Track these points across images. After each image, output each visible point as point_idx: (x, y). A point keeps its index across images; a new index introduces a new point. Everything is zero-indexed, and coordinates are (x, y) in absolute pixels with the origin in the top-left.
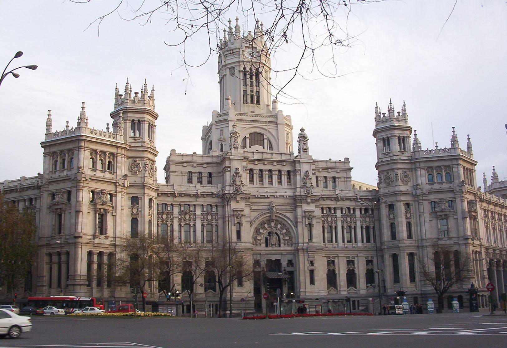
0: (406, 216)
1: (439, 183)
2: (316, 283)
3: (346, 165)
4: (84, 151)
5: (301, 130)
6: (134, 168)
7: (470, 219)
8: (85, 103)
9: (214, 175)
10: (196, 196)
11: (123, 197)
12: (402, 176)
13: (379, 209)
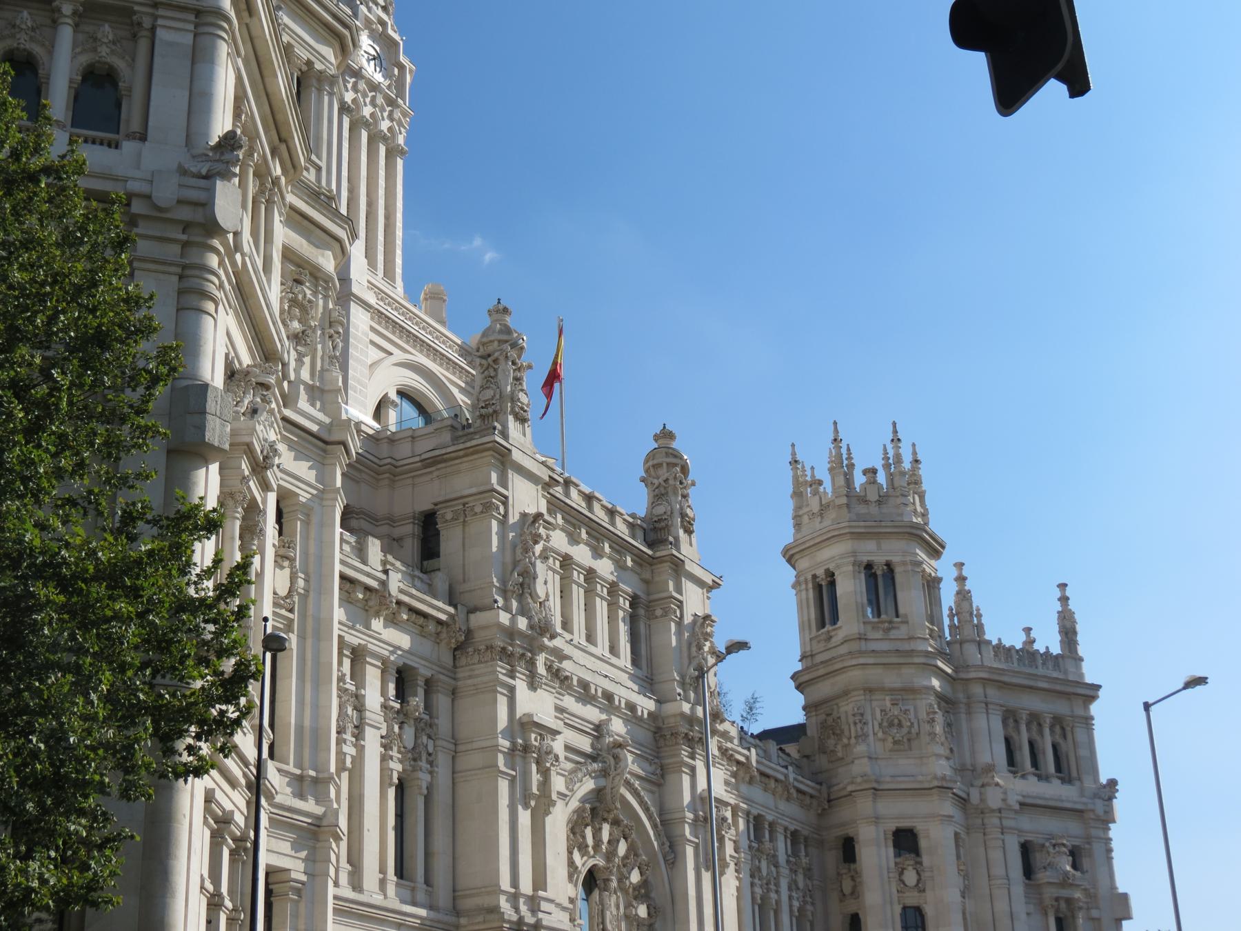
5: (656, 438)
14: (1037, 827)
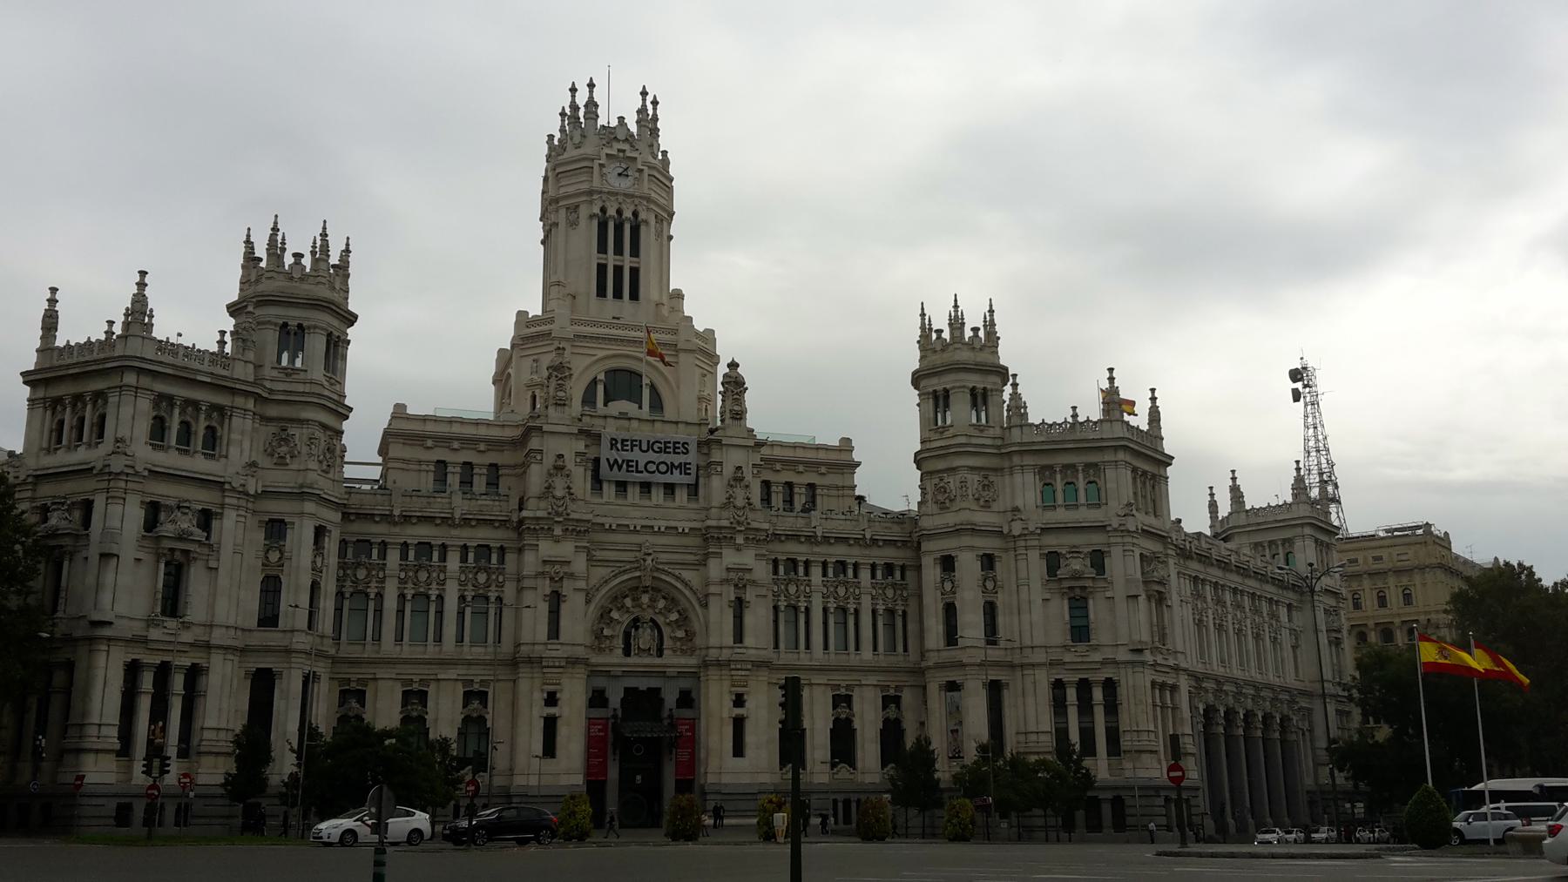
0: (985, 586)
1: (1067, 507)
2: (749, 750)
3: (843, 457)
4: (136, 397)
5: (729, 366)
6: (280, 446)
7: (1149, 598)
8: (147, 273)
9: (507, 471)
10: (447, 521)
11: (243, 520)
12: (976, 486)
13: (919, 568)
14: (1051, 541)
